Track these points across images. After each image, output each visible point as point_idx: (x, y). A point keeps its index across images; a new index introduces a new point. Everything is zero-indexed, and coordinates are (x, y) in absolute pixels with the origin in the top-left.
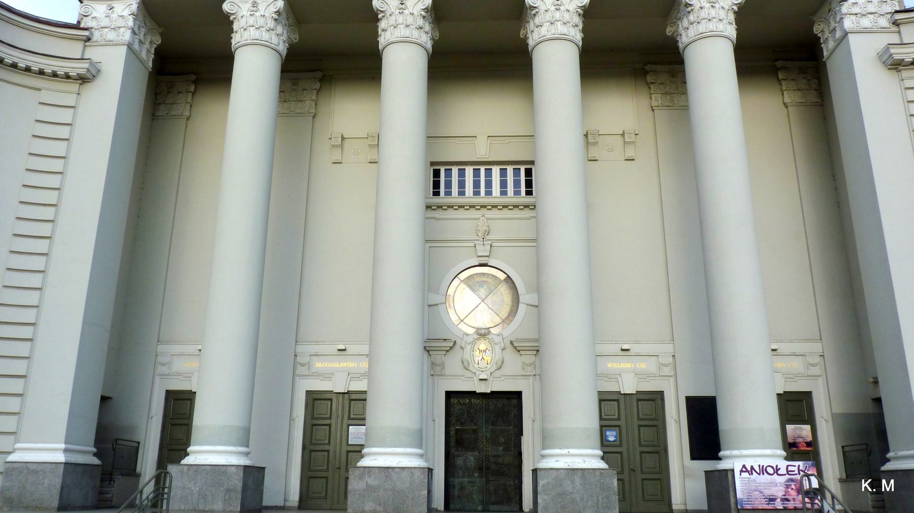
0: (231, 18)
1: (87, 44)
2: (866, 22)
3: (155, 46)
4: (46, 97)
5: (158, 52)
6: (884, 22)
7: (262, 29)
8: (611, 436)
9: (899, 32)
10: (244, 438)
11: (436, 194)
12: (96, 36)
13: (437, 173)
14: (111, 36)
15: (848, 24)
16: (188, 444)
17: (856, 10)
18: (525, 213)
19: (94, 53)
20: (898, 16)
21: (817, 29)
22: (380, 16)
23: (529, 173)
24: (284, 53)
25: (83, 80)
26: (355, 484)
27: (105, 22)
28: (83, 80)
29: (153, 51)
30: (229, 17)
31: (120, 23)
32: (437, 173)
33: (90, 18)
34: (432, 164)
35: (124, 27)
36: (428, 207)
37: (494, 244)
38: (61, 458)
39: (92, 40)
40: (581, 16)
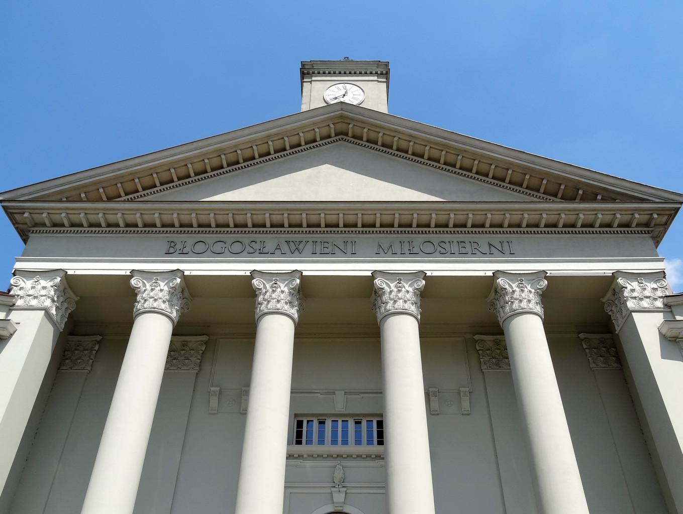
0: (136, 291)
1: (11, 308)
2: (645, 304)
3: (70, 311)
5: (71, 316)
6: (659, 304)
7: (160, 300)
9: (671, 312)
11: (299, 442)
12: (20, 303)
13: (300, 424)
14: (34, 302)
17: (635, 294)
18: (376, 461)
19: (14, 316)
20: (670, 300)
21: (607, 309)
22: (257, 293)
23: (380, 424)
24: (176, 321)
27: (31, 292)
29: (67, 316)
30: (134, 290)
31: (44, 292)
33: (19, 288)
34: (296, 415)
35: (45, 296)
37: (348, 491)
39: (16, 305)
40: (419, 295)
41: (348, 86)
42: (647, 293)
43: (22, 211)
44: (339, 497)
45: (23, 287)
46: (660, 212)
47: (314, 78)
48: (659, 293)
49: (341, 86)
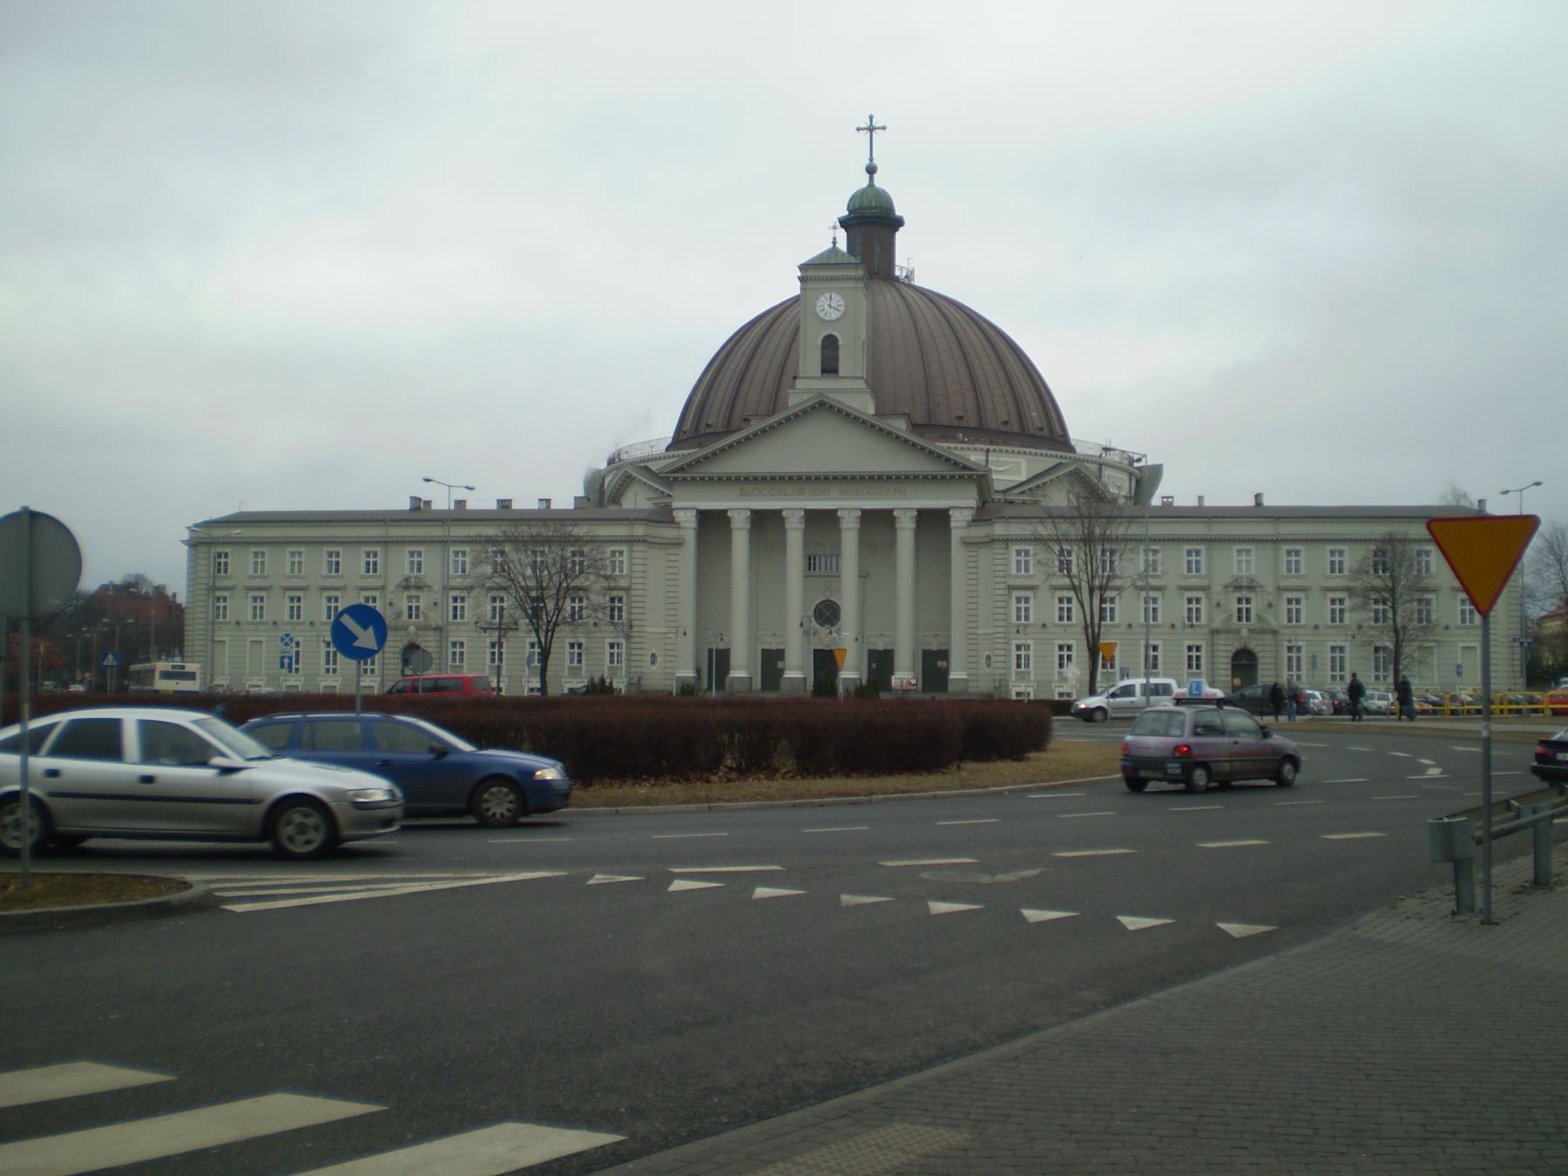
2: (958, 524)
4: (669, 551)
6: (964, 524)
8: (874, 665)
10: (747, 668)
12: (682, 525)
13: (810, 559)
14: (687, 525)
15: (952, 525)
16: (729, 670)
19: (682, 532)
25: (680, 544)
26: (783, 684)
27: (685, 519)
28: (680, 544)
32: (810, 559)
36: (805, 576)
38: (692, 675)
41: (834, 295)
42: (962, 518)
43: (668, 478)
44: (828, 594)
45: (680, 516)
46: (978, 476)
47: (808, 287)
48: (967, 518)
49: (828, 295)
